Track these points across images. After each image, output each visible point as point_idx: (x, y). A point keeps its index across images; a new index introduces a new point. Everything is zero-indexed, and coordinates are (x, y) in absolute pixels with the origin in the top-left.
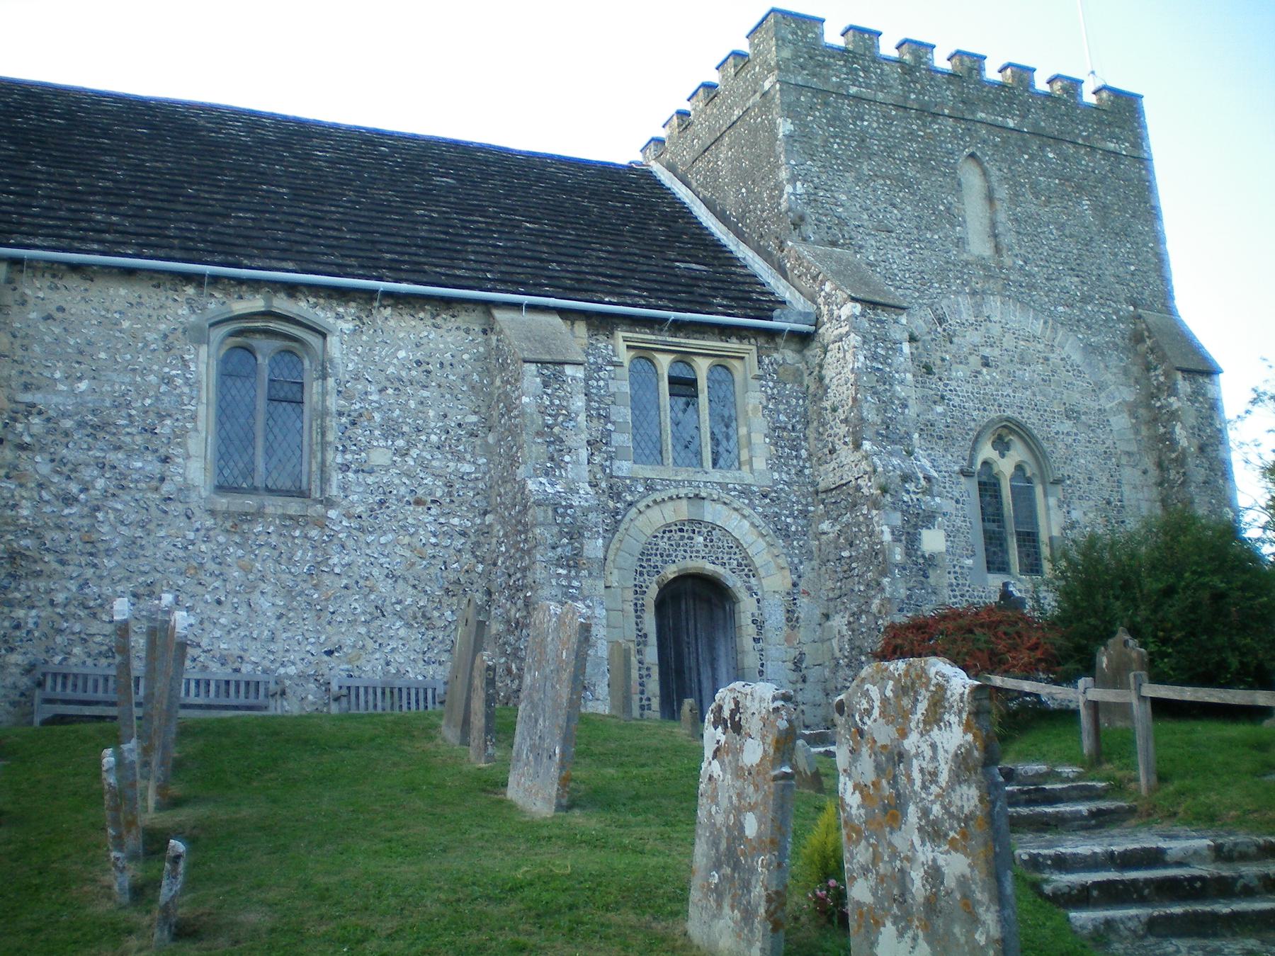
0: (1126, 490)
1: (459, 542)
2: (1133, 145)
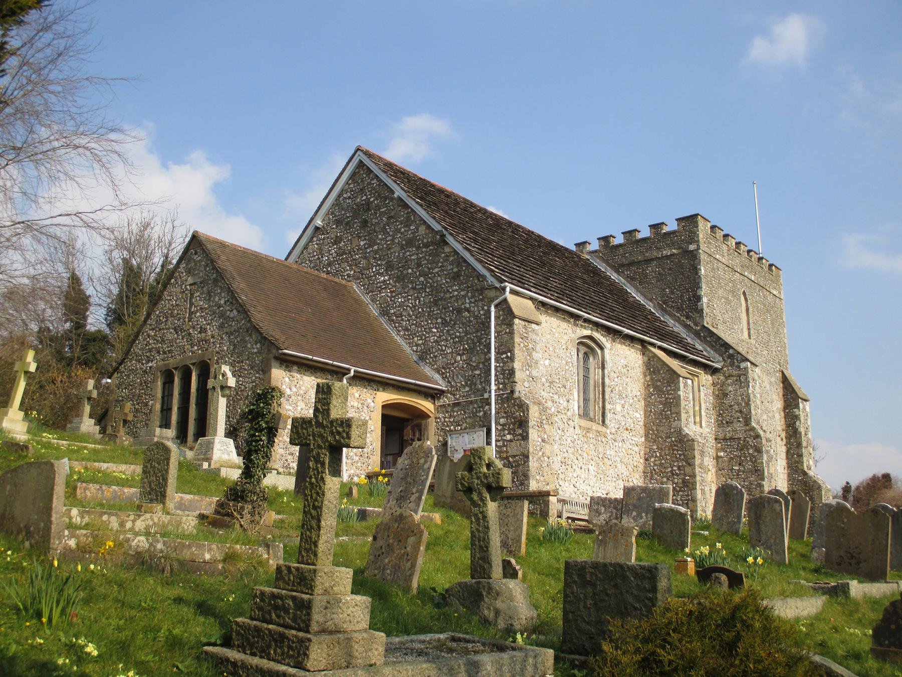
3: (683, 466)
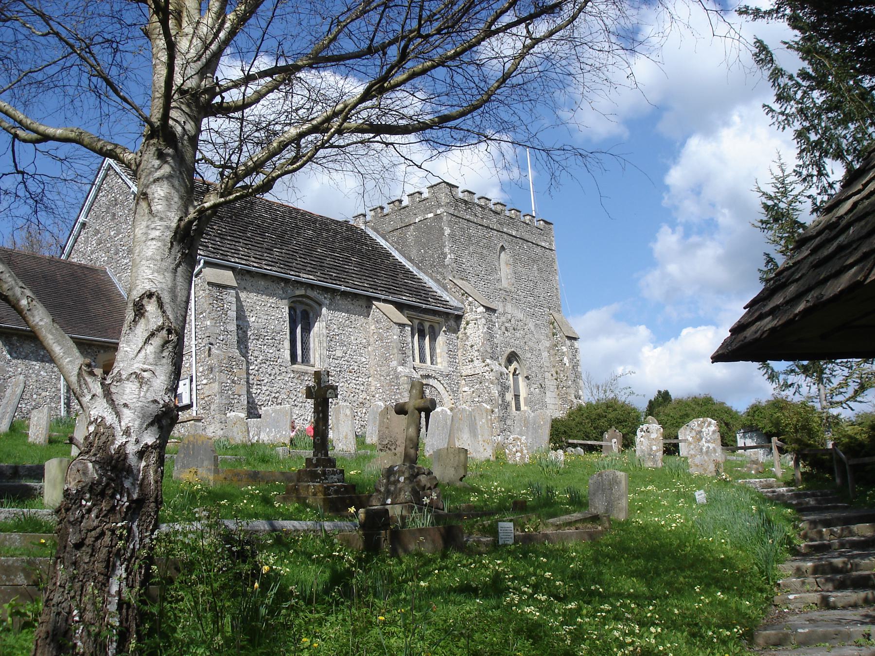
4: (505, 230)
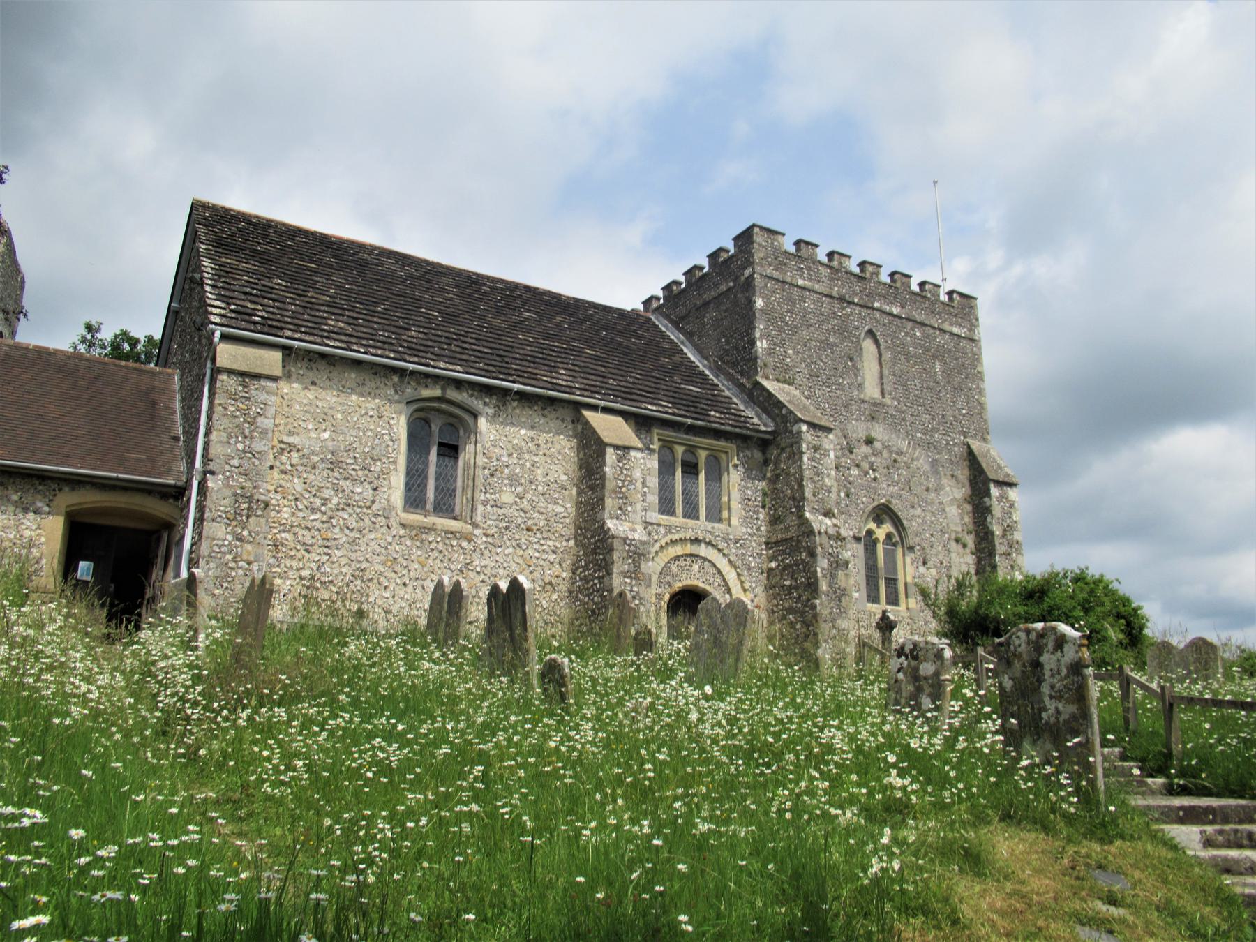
0: (953, 555)
1: (552, 557)
2: (970, 330)
3: (603, 577)
4: (877, 305)
